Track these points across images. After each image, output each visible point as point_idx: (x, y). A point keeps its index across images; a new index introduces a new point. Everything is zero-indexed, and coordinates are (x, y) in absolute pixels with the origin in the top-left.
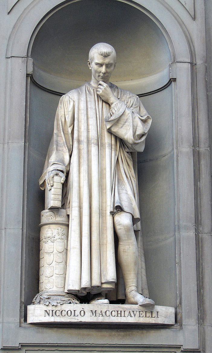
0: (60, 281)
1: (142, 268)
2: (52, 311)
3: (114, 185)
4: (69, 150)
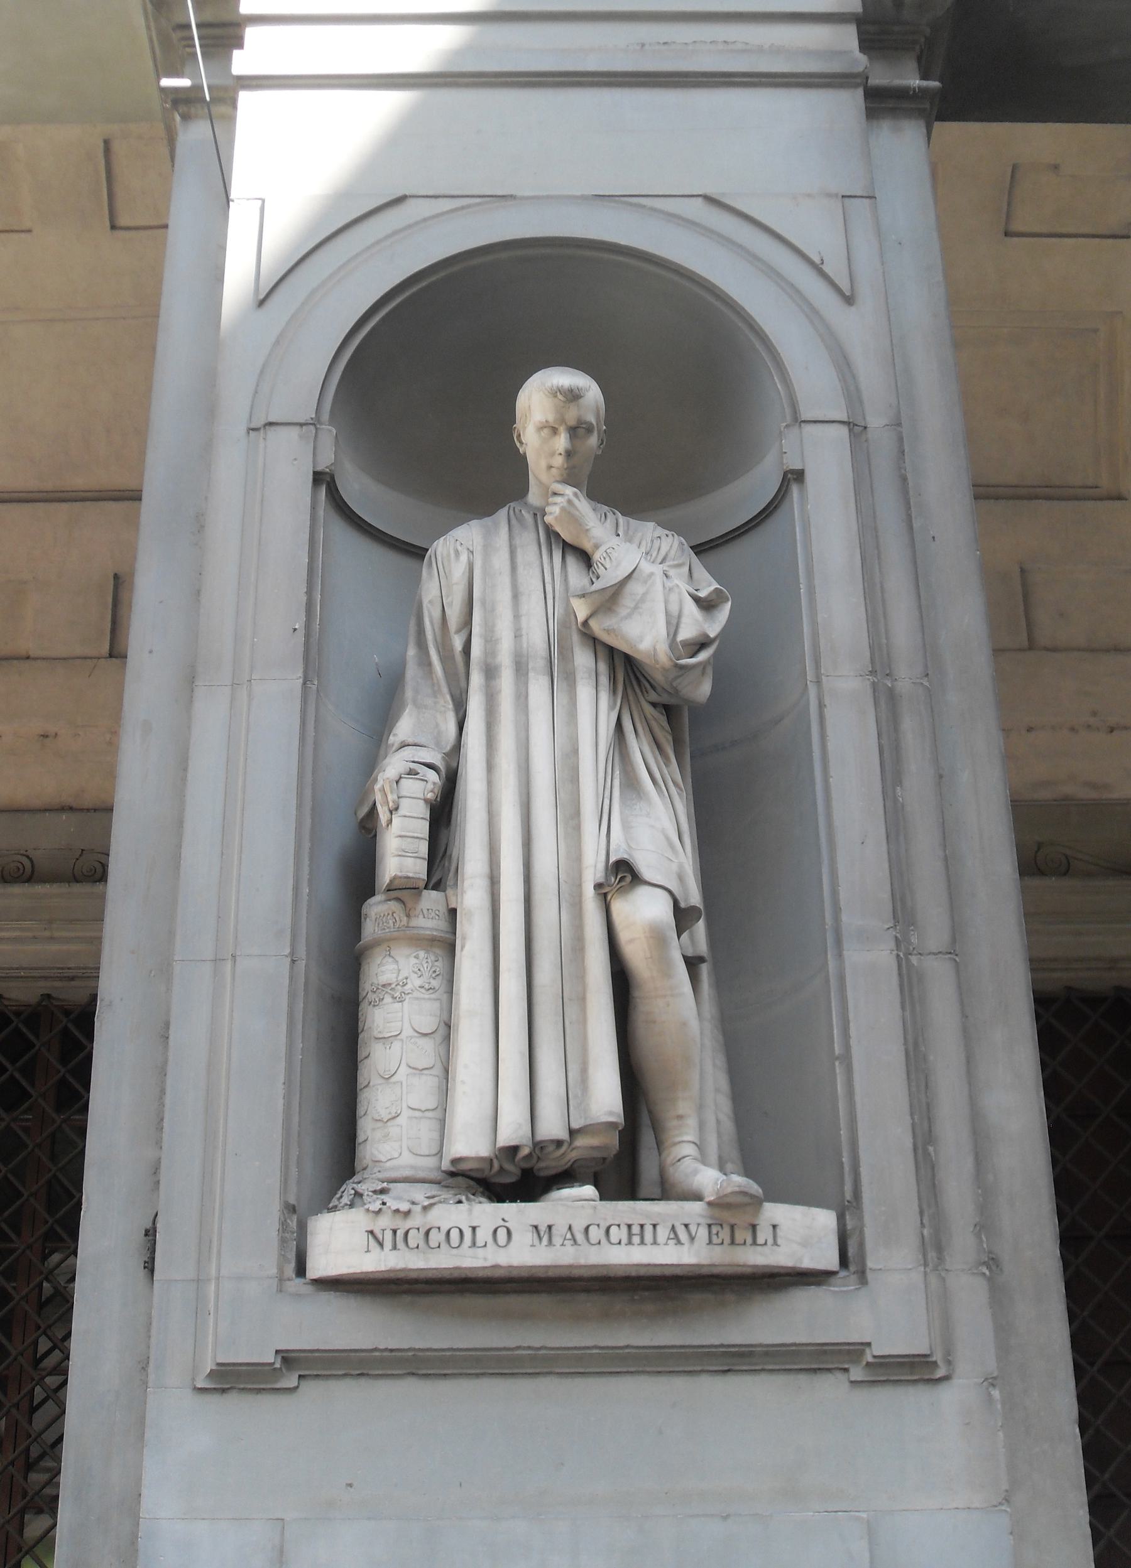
0: (426, 1132)
1: (717, 1090)
2: (395, 1232)
3: (607, 802)
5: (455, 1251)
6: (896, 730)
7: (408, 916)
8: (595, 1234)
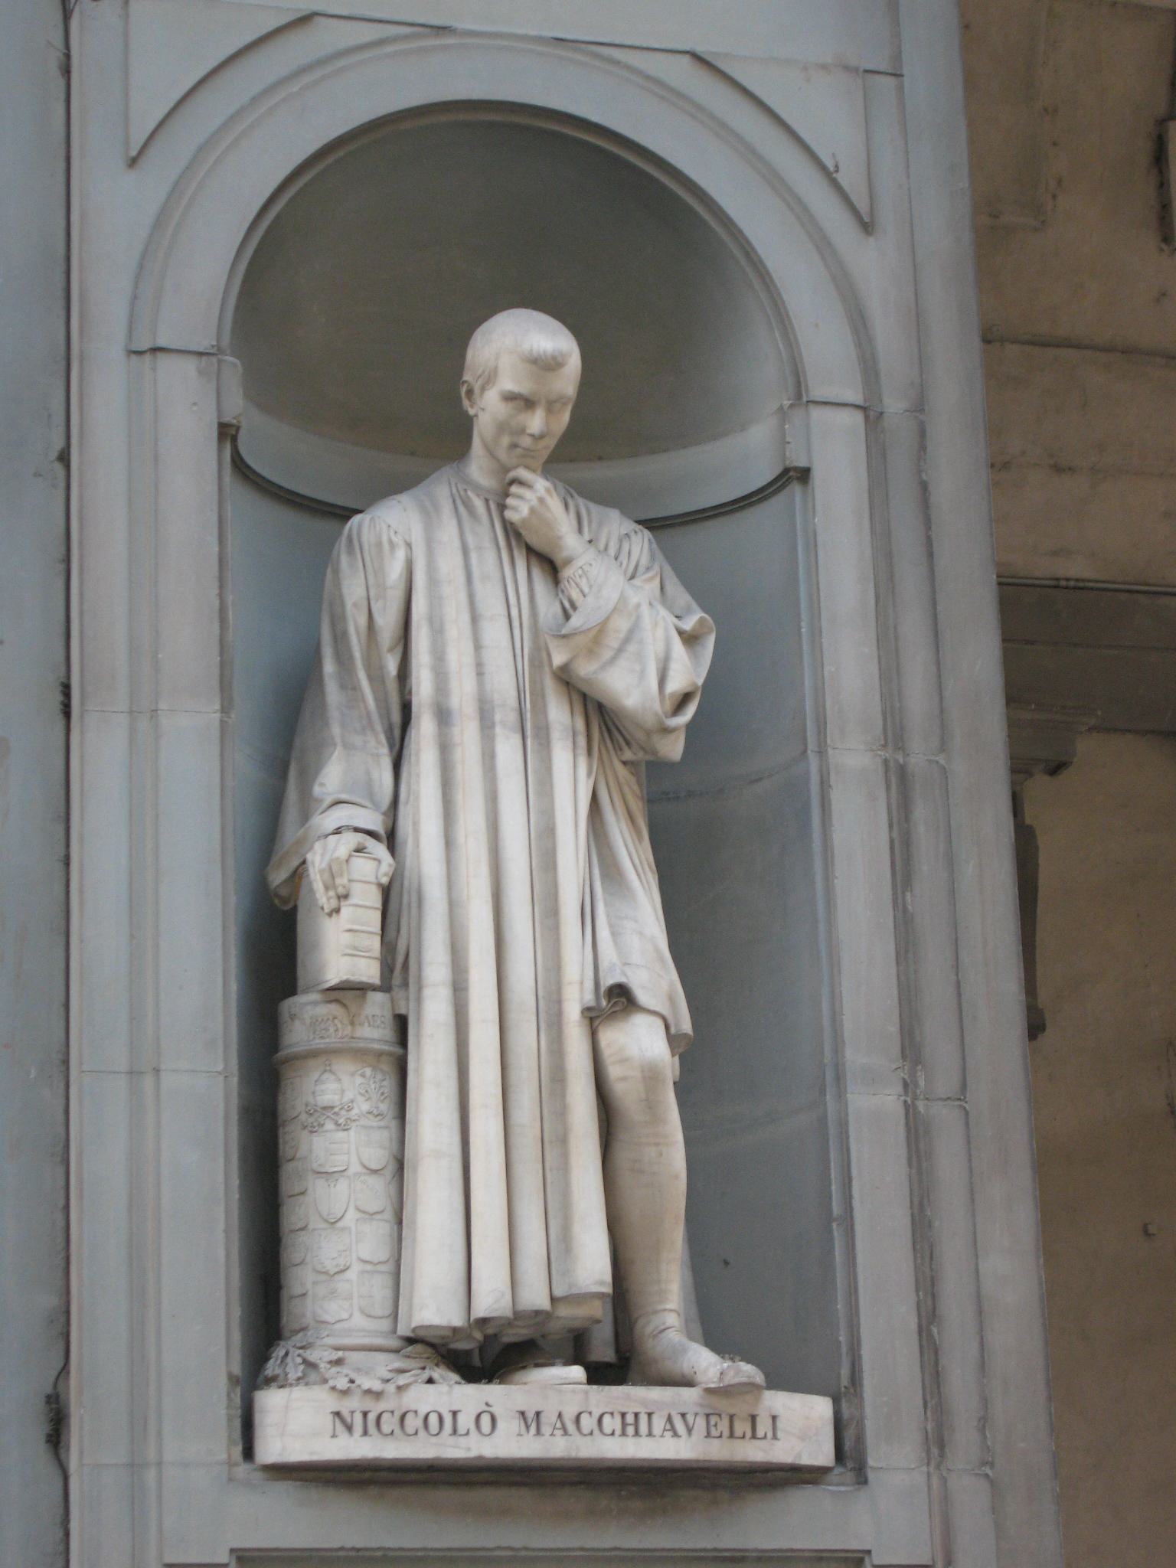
0: (379, 1289)
2: (365, 1414)
4: (391, 746)
5: (434, 1440)
6: (907, 819)
7: (352, 1024)
8: (587, 1423)
